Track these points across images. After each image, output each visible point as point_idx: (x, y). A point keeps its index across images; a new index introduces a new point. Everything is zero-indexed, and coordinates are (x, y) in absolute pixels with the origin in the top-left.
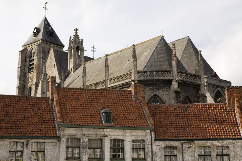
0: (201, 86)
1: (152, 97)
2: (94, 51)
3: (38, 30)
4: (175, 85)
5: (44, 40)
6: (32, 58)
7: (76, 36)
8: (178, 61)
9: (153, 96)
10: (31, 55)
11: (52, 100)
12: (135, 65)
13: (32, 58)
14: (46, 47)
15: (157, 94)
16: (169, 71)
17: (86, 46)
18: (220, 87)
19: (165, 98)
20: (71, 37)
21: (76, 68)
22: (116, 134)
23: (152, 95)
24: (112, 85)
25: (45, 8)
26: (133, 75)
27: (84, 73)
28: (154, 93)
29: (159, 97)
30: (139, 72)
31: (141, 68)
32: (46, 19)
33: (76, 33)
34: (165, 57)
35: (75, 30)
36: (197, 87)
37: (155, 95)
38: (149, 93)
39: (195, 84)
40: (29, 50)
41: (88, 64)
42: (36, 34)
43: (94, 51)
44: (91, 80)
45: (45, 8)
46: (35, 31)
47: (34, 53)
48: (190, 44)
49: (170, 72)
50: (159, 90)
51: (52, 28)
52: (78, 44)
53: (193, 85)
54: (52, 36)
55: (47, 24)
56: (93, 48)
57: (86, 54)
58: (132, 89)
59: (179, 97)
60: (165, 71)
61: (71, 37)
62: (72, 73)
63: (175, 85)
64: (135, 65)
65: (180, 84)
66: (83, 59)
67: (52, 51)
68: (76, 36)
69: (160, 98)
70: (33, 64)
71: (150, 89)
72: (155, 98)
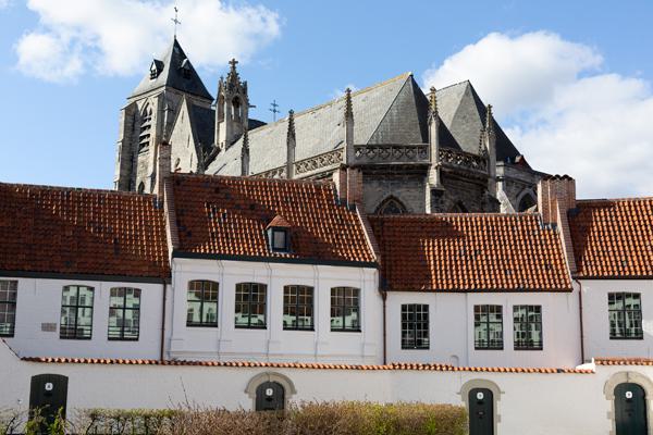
0: (490, 180)
1: (383, 202)
2: (275, 111)
3: (160, 65)
4: (433, 177)
5: (171, 83)
6: (147, 123)
7: (234, 76)
8: (441, 127)
9: (387, 199)
10: (145, 116)
11: (162, 204)
12: (350, 135)
13: (147, 123)
15: (395, 195)
16: (420, 147)
17: (252, 96)
18: (530, 187)
19: (412, 205)
20: (222, 78)
21: (230, 143)
22: (301, 274)
23: (385, 197)
24: (301, 175)
25: (176, 21)
26: (344, 154)
27: (246, 151)
28: (390, 193)
29: (398, 201)
30: (358, 148)
31: (362, 137)
32: (176, 44)
33: (234, 68)
34: (414, 117)
35: (230, 62)
36: (483, 184)
37: (392, 197)
38: (376, 193)
39: (477, 176)
40: (140, 107)
41: (253, 135)
42: (154, 75)
43: (275, 111)
44: (256, 168)
45: (176, 21)
46: (154, 67)
47: (151, 114)
48: (472, 97)
49: (425, 150)
50: (399, 187)
51: (188, 62)
52: (238, 91)
53: (473, 178)
55: (178, 53)
56: (275, 105)
57: (253, 114)
58: (336, 177)
59: (442, 202)
60: (414, 147)
61: (222, 78)
62: (223, 152)
63: (433, 177)
64: (350, 135)
65: (442, 175)
66: (246, 124)
69: (401, 203)
70: (149, 135)
71: (380, 184)
72: (392, 204)
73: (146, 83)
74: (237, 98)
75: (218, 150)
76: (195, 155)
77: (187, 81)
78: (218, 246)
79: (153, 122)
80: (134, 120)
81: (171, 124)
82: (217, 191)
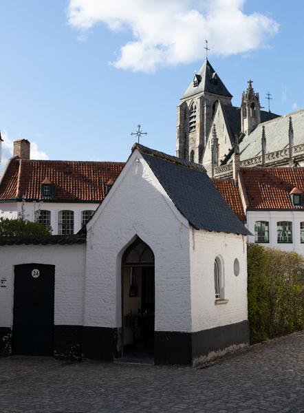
2: (269, 98)
3: (199, 78)
5: (207, 89)
6: (193, 114)
7: (251, 90)
10: (192, 110)
11: (237, 183)
13: (193, 114)
14: (212, 98)
21: (251, 130)
24: (298, 154)
25: (207, 49)
27: (264, 139)
41: (270, 125)
42: (196, 84)
45: (207, 49)
46: (196, 79)
47: (195, 108)
51: (216, 74)
54: (217, 85)
62: (246, 137)
67: (219, 108)
68: (251, 90)
70: (195, 122)
73: (191, 89)
74: (253, 104)
75: (244, 135)
76: (228, 136)
77: (216, 87)
78: (267, 204)
79: (198, 113)
80: (186, 112)
81: (214, 114)
82: (264, 175)
